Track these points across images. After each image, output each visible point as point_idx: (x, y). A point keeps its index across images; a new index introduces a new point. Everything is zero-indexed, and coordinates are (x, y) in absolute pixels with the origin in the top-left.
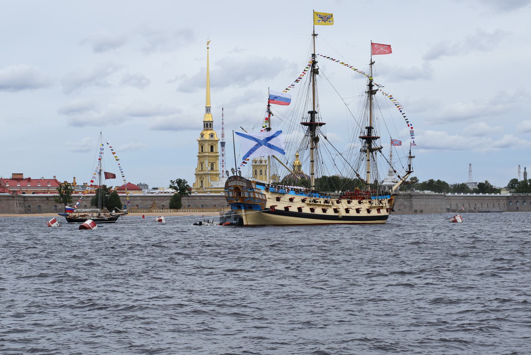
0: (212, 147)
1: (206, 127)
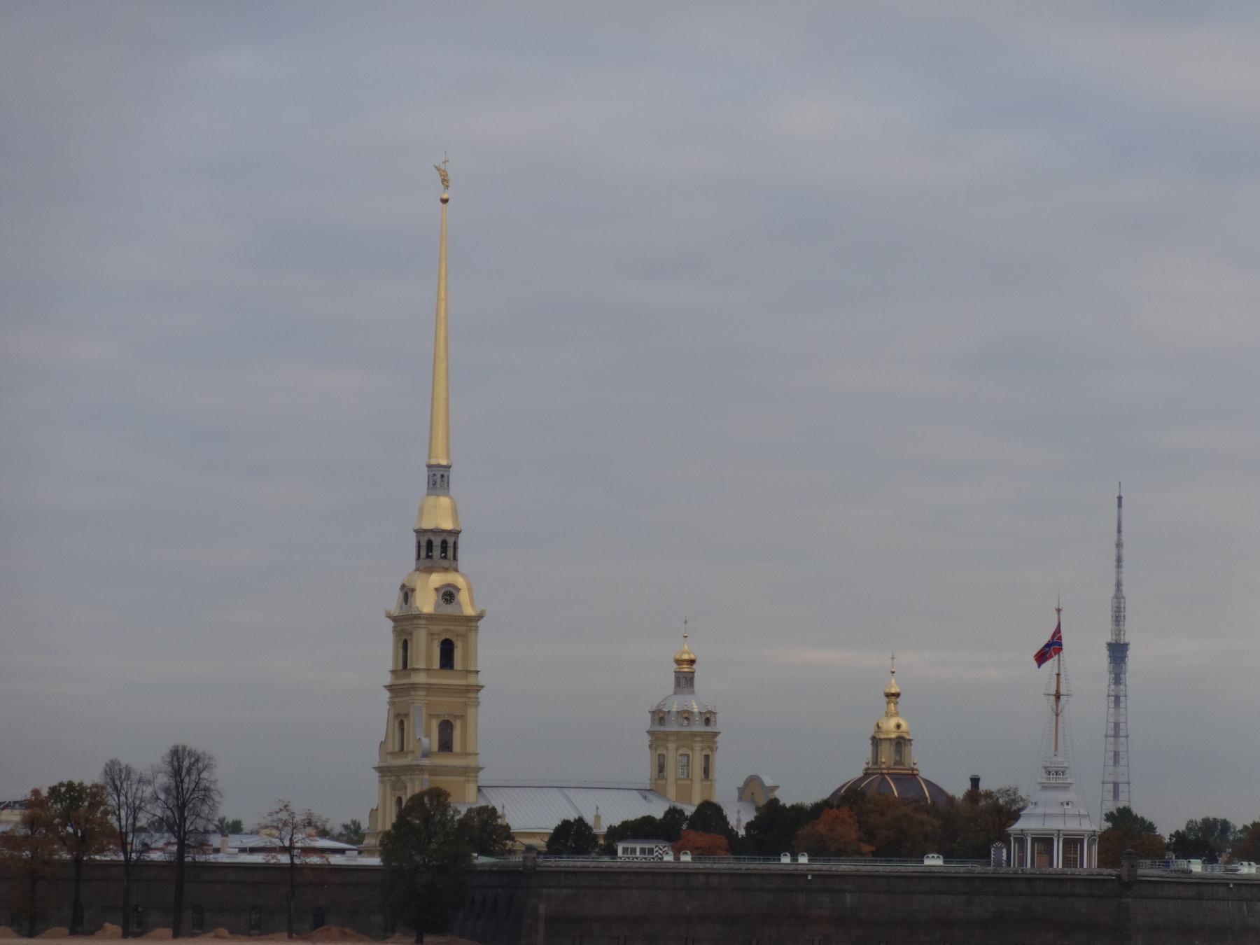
0: (447, 650)
1: (423, 554)
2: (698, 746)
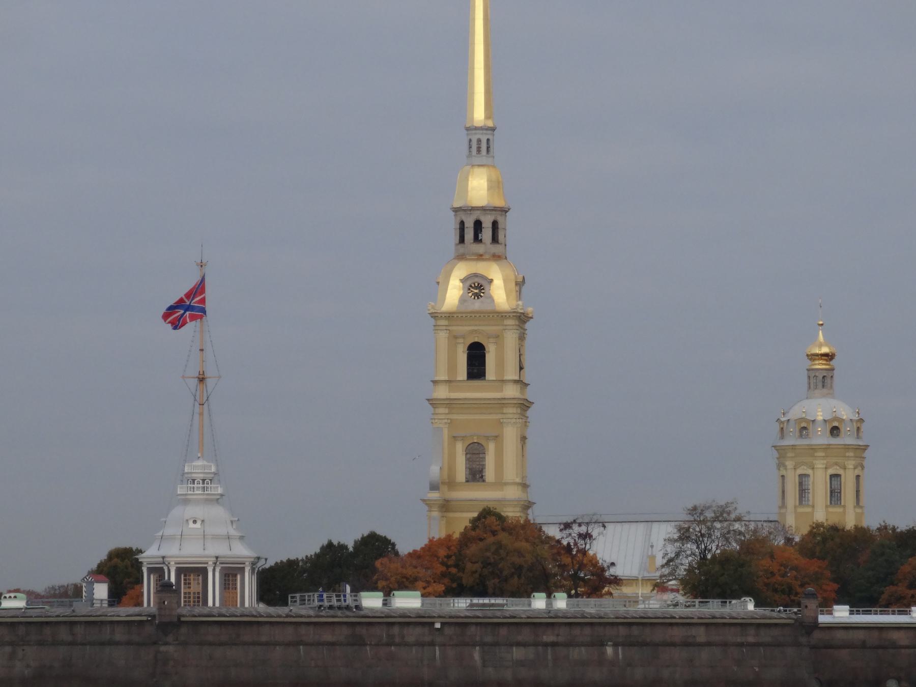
2: (820, 464)
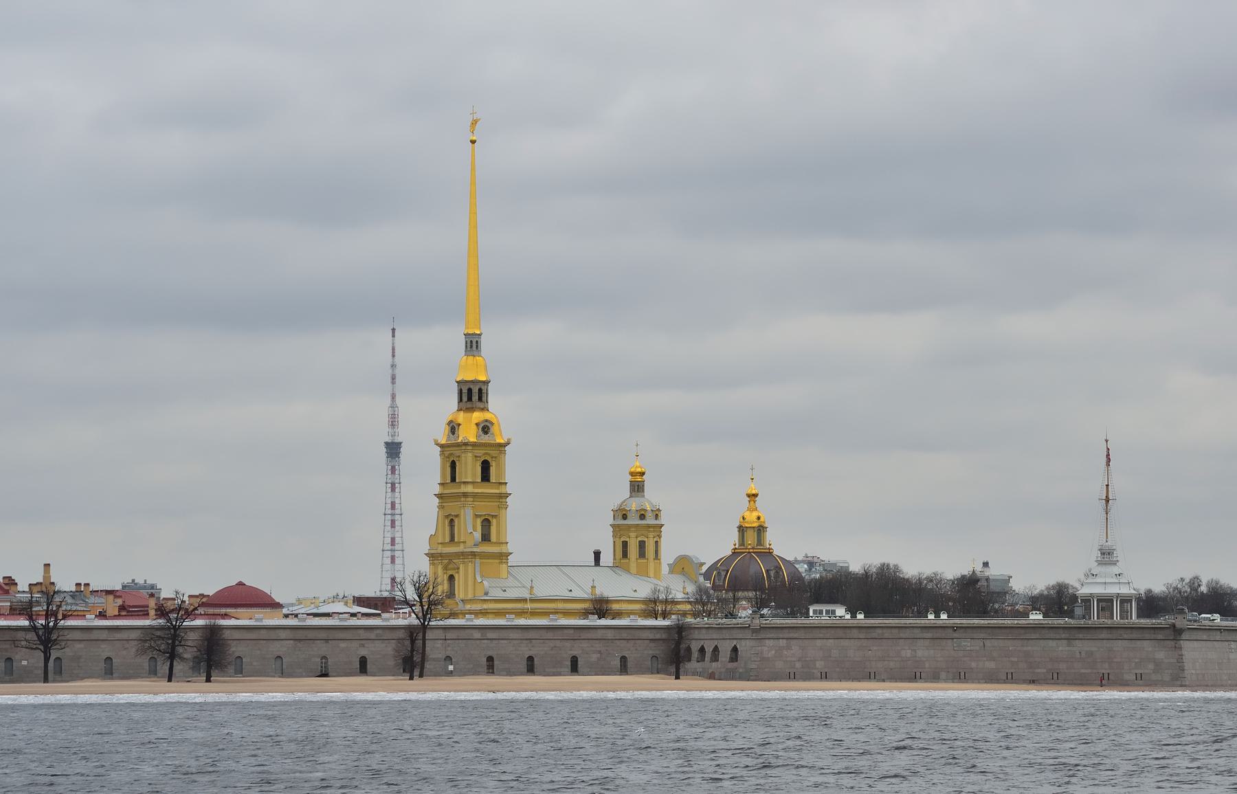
0: (486, 467)
1: (465, 398)
